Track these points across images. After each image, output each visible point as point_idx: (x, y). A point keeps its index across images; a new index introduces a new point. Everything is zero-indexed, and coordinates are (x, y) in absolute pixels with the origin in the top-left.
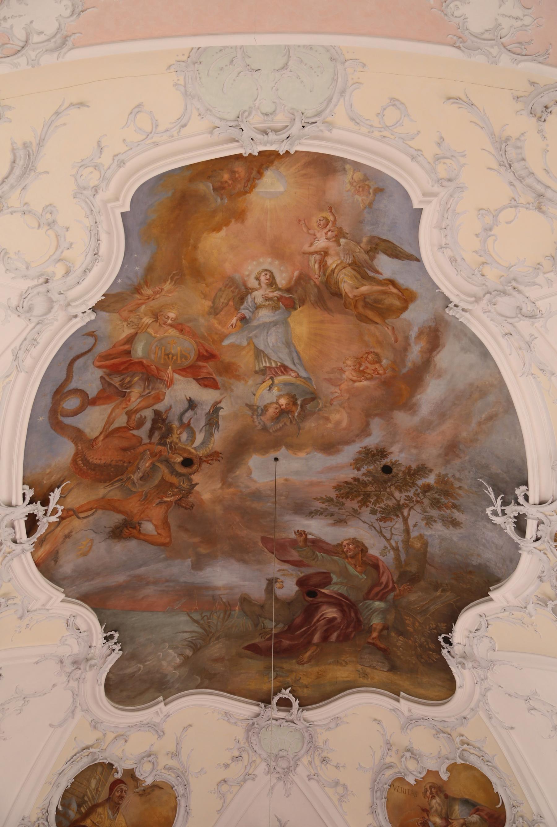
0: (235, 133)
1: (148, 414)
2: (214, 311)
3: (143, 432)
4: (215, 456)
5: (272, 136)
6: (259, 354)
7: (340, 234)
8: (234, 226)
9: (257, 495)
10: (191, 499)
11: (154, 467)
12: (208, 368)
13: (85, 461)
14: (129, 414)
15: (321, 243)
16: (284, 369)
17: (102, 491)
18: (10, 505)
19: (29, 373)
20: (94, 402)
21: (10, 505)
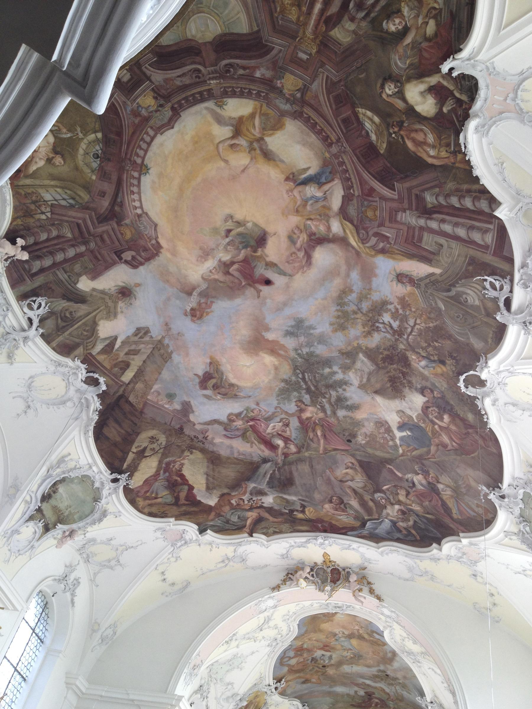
0: (326, 607)
1: (310, 658)
2: (327, 638)
3: (309, 662)
4: (332, 665)
5: (338, 609)
6: (342, 646)
7: (362, 627)
8: (330, 622)
9: (347, 673)
10: (326, 674)
11: (313, 668)
12: (327, 648)
13: (292, 670)
14: (304, 659)
15: (357, 628)
16: (351, 650)
17: (298, 675)
18: (269, 685)
19: (272, 658)
20: (293, 658)
21: (269, 685)
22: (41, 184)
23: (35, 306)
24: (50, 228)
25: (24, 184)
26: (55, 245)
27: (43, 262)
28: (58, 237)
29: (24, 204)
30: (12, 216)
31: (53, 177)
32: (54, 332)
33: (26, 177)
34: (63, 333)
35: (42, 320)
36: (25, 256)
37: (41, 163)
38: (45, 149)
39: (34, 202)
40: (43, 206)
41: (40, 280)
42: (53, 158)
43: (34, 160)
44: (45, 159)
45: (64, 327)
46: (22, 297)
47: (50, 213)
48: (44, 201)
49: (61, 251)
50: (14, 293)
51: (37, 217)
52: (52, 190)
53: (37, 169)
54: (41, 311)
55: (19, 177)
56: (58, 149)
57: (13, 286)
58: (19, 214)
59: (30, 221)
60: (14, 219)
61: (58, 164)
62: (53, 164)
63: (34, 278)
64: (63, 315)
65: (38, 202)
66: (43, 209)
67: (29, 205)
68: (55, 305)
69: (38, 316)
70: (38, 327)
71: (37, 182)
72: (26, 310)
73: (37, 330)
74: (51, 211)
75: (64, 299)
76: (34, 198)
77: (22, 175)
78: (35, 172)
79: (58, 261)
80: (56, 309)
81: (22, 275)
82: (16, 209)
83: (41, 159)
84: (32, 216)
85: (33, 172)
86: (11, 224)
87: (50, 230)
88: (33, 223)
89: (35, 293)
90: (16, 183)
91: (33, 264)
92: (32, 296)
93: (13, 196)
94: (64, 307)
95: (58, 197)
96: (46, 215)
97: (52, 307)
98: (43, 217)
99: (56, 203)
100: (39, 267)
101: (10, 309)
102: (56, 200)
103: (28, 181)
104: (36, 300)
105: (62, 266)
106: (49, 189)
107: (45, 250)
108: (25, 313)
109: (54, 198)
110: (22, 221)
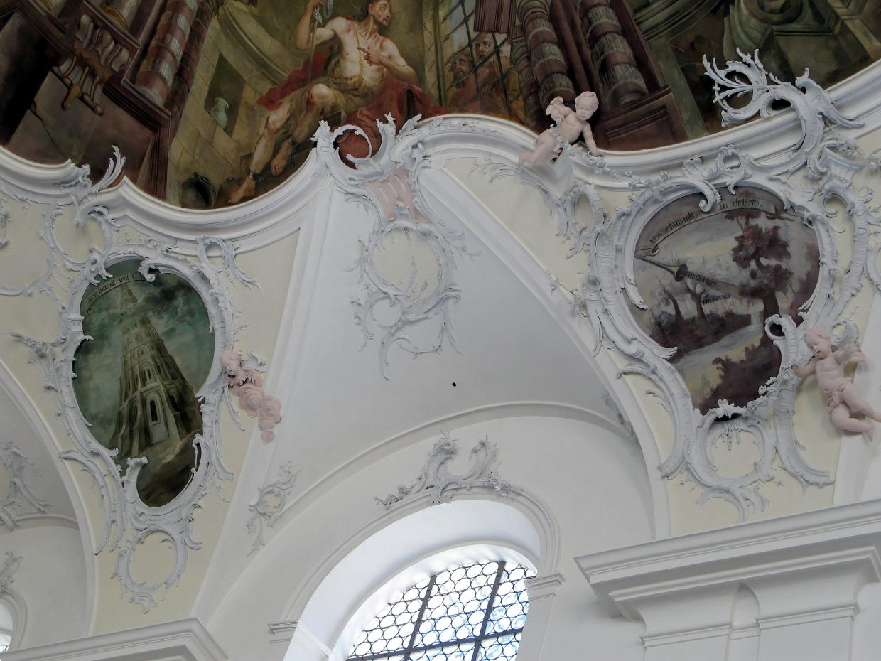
22: (433, 48)
23: (740, 87)
24: (531, 36)
25: (436, 84)
26: (573, 26)
27: (619, 57)
28: (553, 19)
29: (478, 90)
30: (504, 117)
31: (416, 25)
32: (832, 44)
33: (421, 79)
34: (837, 17)
35: (788, 75)
36: (587, 101)
37: (391, 48)
38: (361, 38)
39: (474, 69)
40: (480, 49)
41: (668, 70)
42: (376, 22)
43: (384, 60)
44: (381, 38)
45: (818, 16)
46: (710, 117)
47: (497, 35)
48: (470, 45)
49: (590, 14)
50: (696, 136)
51: (505, 64)
52: (446, 28)
53: (403, 55)
54: (757, 75)
55: (423, 94)
56: (358, 9)
57: (676, 136)
58: (501, 104)
59: (517, 80)
60: (512, 116)
61: (387, 12)
62: (390, 23)
63: (661, 84)
64: (776, 17)
65: (472, 58)
66: (488, 50)
67: (480, 80)
68: (743, 36)
69: (770, 82)
70: (793, 84)
71: (430, 57)
72: (746, 112)
73: (804, 90)
74: (493, 32)
75: (727, 13)
76: (465, 68)
77: (417, 88)
78: (409, 61)
79: (615, 22)
80: (756, 35)
81: (651, 112)
82: (490, 109)
83: (381, 47)
84: (505, 76)
85: (409, 63)
86: (522, 123)
87: (536, 37)
88: (520, 73)
89: (703, 87)
90: (434, 103)
91: (621, 82)
92: (712, 94)
93: (462, 111)
94: (752, 14)
95: (458, 15)
96: (503, 43)
97: (749, 43)
98: (506, 50)
99: (471, 22)
100: (632, 70)
101: (730, 151)
102: (466, 20)
103: (430, 77)
104: (719, 85)
105: (631, 12)
106: (443, 36)
107: (588, 52)
108: (757, 115)
109: (462, 24)
110: (517, 98)
